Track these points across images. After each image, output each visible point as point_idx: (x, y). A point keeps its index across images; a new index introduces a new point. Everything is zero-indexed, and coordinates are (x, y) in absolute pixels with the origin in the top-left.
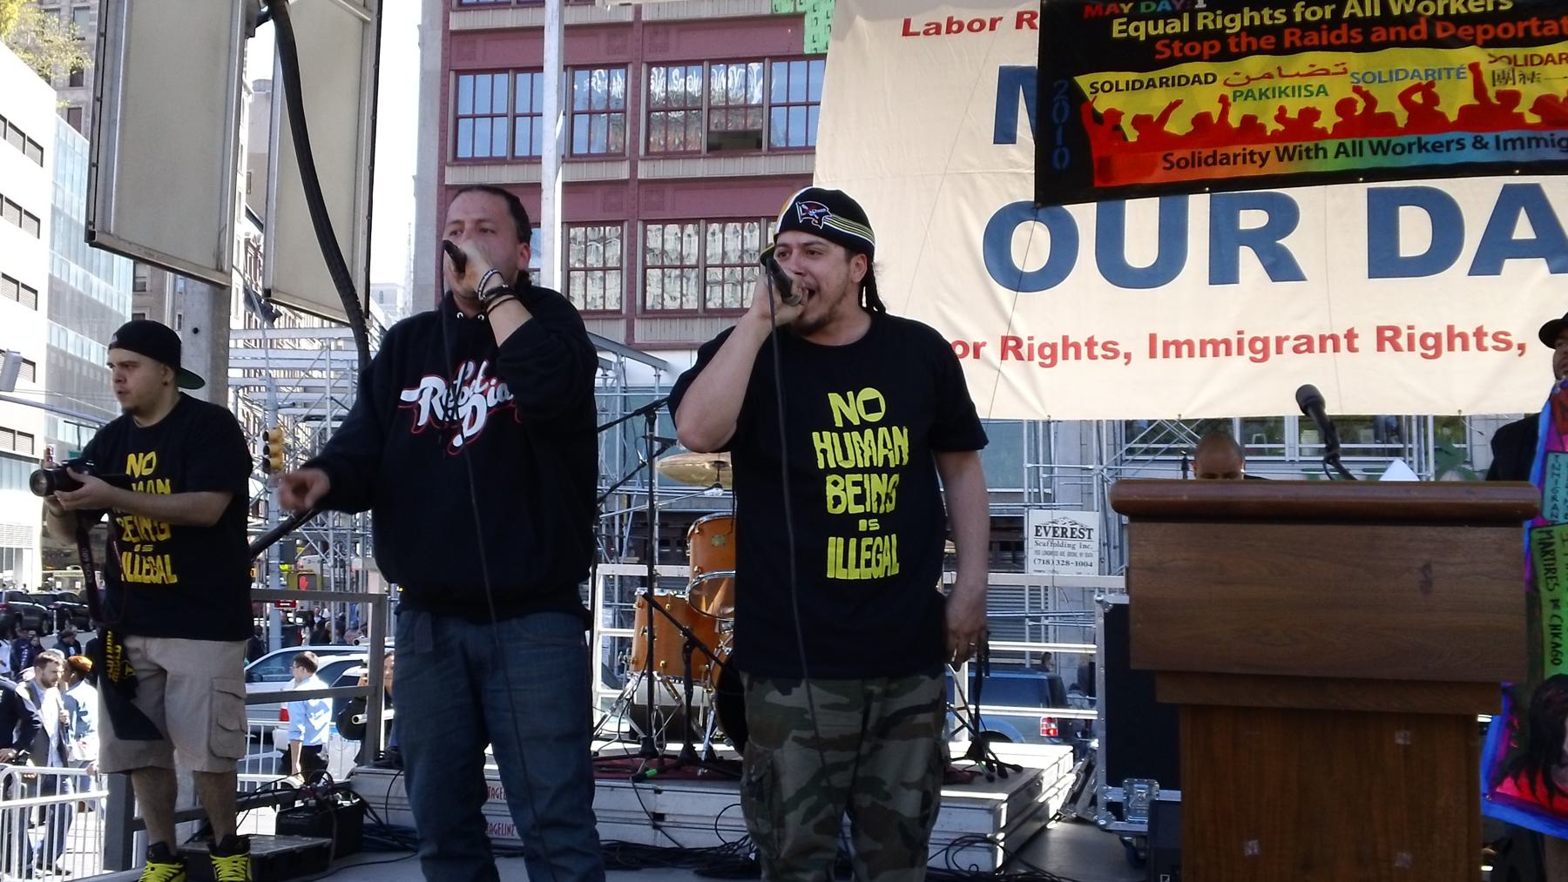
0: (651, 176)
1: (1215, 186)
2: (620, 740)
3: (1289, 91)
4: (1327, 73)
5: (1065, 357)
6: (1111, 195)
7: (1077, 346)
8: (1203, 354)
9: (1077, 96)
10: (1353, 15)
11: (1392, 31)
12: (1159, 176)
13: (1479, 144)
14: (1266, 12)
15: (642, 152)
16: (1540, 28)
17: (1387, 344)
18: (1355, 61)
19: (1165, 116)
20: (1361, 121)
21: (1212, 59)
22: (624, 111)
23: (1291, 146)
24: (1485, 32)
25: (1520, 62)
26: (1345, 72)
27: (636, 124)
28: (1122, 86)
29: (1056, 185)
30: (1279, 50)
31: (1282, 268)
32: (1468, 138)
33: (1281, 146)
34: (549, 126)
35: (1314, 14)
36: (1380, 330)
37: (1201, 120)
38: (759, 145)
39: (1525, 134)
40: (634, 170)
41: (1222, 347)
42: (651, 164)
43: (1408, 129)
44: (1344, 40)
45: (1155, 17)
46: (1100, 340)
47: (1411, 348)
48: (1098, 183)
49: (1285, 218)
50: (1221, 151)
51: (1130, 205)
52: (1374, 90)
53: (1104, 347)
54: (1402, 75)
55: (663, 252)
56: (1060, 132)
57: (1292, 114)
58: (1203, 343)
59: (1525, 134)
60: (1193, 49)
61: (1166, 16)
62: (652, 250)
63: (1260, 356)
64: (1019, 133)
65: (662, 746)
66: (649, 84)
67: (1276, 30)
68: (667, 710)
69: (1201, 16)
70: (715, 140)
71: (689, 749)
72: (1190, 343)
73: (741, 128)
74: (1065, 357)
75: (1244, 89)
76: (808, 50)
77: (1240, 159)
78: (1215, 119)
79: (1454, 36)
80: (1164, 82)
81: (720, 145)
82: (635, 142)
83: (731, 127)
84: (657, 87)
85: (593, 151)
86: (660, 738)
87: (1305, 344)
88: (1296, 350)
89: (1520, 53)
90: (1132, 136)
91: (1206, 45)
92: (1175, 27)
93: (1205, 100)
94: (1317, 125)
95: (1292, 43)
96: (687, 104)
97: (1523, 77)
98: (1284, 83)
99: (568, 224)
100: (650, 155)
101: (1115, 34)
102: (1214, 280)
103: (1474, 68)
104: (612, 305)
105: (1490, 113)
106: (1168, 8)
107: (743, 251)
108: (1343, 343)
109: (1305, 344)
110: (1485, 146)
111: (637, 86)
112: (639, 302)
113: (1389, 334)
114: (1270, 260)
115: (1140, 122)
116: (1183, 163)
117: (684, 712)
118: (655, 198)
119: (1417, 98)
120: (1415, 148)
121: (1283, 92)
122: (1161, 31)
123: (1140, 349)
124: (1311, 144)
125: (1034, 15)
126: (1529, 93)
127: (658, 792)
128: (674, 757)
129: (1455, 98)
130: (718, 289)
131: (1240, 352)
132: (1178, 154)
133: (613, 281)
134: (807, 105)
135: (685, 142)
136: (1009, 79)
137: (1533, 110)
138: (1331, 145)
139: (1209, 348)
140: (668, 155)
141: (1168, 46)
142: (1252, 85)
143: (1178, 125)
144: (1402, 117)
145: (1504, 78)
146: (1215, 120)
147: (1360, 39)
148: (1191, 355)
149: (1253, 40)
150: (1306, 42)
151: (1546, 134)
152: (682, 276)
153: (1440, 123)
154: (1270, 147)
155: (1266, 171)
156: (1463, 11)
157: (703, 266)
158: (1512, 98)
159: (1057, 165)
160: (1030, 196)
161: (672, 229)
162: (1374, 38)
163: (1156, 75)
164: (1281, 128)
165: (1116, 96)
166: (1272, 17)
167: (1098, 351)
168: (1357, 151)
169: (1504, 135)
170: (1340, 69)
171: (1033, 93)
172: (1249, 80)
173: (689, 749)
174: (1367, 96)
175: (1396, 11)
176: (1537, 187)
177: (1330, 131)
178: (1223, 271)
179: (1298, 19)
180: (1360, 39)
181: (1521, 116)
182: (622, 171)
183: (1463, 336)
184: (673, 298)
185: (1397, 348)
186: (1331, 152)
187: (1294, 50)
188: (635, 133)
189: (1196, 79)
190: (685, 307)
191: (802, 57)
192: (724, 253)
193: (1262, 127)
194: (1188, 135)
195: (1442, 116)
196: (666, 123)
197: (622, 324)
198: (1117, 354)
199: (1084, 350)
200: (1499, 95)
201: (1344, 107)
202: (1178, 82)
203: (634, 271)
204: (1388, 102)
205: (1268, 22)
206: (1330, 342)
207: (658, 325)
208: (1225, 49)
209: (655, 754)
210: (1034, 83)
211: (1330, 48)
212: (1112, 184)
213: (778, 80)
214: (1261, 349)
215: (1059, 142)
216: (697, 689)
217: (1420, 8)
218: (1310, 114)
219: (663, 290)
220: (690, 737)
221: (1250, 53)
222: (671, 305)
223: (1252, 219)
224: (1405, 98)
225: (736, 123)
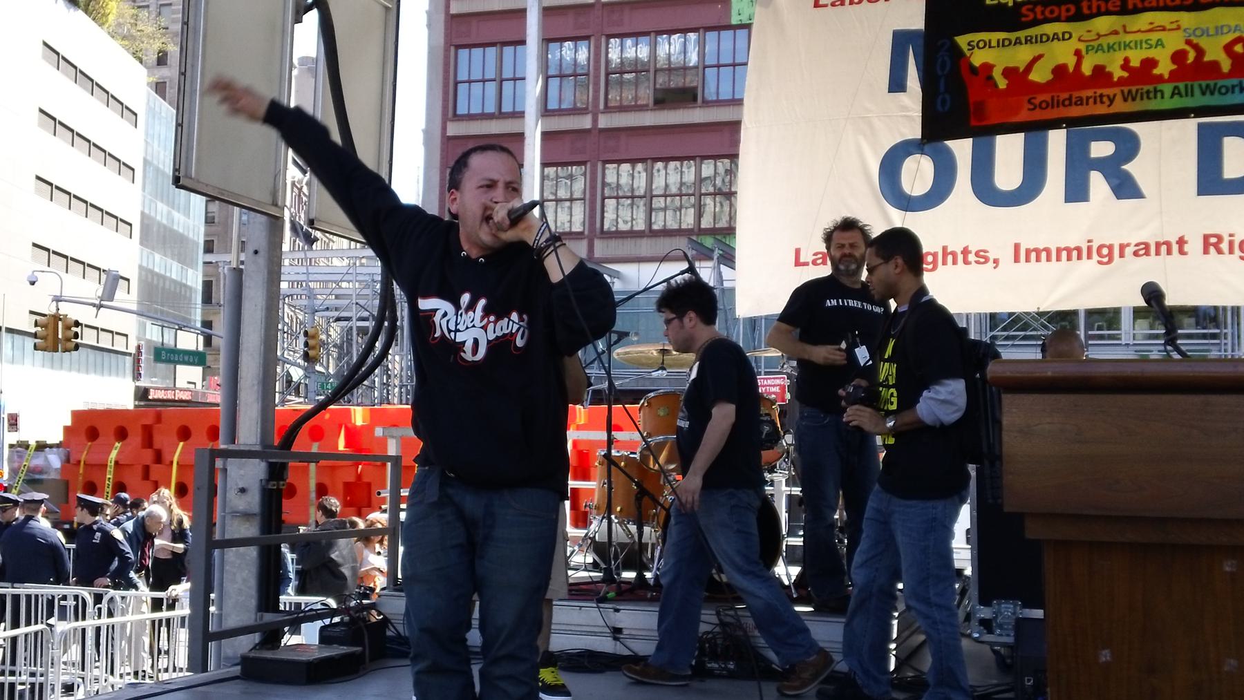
0: (609, 125)
1: (1070, 123)
2: (586, 570)
3: (1132, 45)
4: (1164, 29)
5: (944, 263)
7: (954, 254)
8: (1059, 259)
9: (957, 53)
12: (1024, 116)
15: (602, 106)
17: (1212, 249)
18: (1187, 19)
19: (1029, 67)
20: (1192, 68)
21: (1069, 19)
23: (1134, 89)
26: (1178, 28)
27: (597, 84)
28: (994, 43)
29: (941, 123)
31: (1125, 188)
33: (1126, 90)
34: (530, 85)
36: (1206, 238)
37: (1060, 70)
38: (695, 99)
40: (595, 121)
41: (1075, 253)
43: (1230, 75)
46: (973, 249)
47: (1231, 251)
48: (973, 123)
49: (1129, 147)
50: (1076, 94)
52: (1203, 42)
53: (977, 254)
54: (1225, 30)
55: (618, 186)
57: (1135, 63)
58: (1059, 251)
60: (1052, 12)
62: (609, 185)
63: (1106, 260)
65: (619, 575)
66: (607, 53)
68: (623, 546)
70: (660, 96)
71: (641, 577)
72: (1048, 251)
73: (680, 85)
74: (944, 263)
75: (1095, 44)
76: (734, 21)
77: (1091, 101)
78: (1071, 69)
80: (1028, 40)
81: (665, 99)
82: (596, 98)
83: (672, 85)
84: (614, 55)
85: (563, 107)
86: (617, 568)
87: (1143, 249)
88: (1136, 254)
90: (1002, 84)
91: (1063, 8)
93: (1063, 54)
94: (1156, 71)
95: (1135, 5)
96: (637, 67)
98: (1129, 38)
99: (544, 165)
100: (608, 109)
102: (1068, 199)
104: (577, 228)
107: (682, 184)
108: (1175, 248)
109: (1143, 249)
111: (598, 55)
112: (598, 225)
113: (1213, 240)
114: (1116, 182)
115: (1009, 72)
116: (1044, 105)
117: (637, 547)
120: (1237, 90)
121: (1127, 46)
123: (1007, 255)
124: (1151, 88)
127: (617, 610)
128: (629, 583)
130: (661, 214)
131: (1089, 257)
132: (1040, 98)
133: (578, 209)
134: (734, 65)
135: (636, 98)
136: (901, 40)
138: (1167, 88)
139: (1064, 254)
140: (622, 109)
141: (1032, 10)
142: (1101, 41)
143: (1040, 75)
144: (1226, 65)
146: (1071, 69)
148: (1049, 259)
152: (632, 205)
154: (1116, 90)
155: (1112, 110)
157: (649, 196)
159: (939, 108)
160: (918, 134)
161: (626, 167)
163: (1022, 34)
164: (1125, 74)
165: (988, 51)
167: (971, 257)
168: (1189, 92)
170: (1174, 26)
171: (921, 50)
172: (1099, 36)
173: (641, 577)
174: (1196, 47)
177: (1166, 76)
178: (1076, 191)
182: (585, 122)
184: (625, 222)
185: (1220, 252)
186: (1168, 93)
187: (1136, 11)
188: (596, 91)
189: (1056, 37)
190: (635, 228)
191: (729, 27)
192: (667, 186)
193: (1110, 75)
194: (1049, 83)
196: (621, 83)
197: (584, 243)
198: (987, 260)
199: (960, 257)
201: (1178, 57)
202: (1040, 39)
203: (594, 201)
204: (1215, 52)
206: (1163, 247)
207: (613, 243)
209: (614, 581)
210: (921, 42)
212: (984, 123)
213: (710, 47)
214: (1106, 254)
215: (942, 89)
216: (647, 529)
218: (1150, 63)
219: (617, 216)
220: (641, 567)
221: (1099, 14)
222: (623, 227)
223: (1101, 149)
224: (1228, 48)
225: (676, 82)
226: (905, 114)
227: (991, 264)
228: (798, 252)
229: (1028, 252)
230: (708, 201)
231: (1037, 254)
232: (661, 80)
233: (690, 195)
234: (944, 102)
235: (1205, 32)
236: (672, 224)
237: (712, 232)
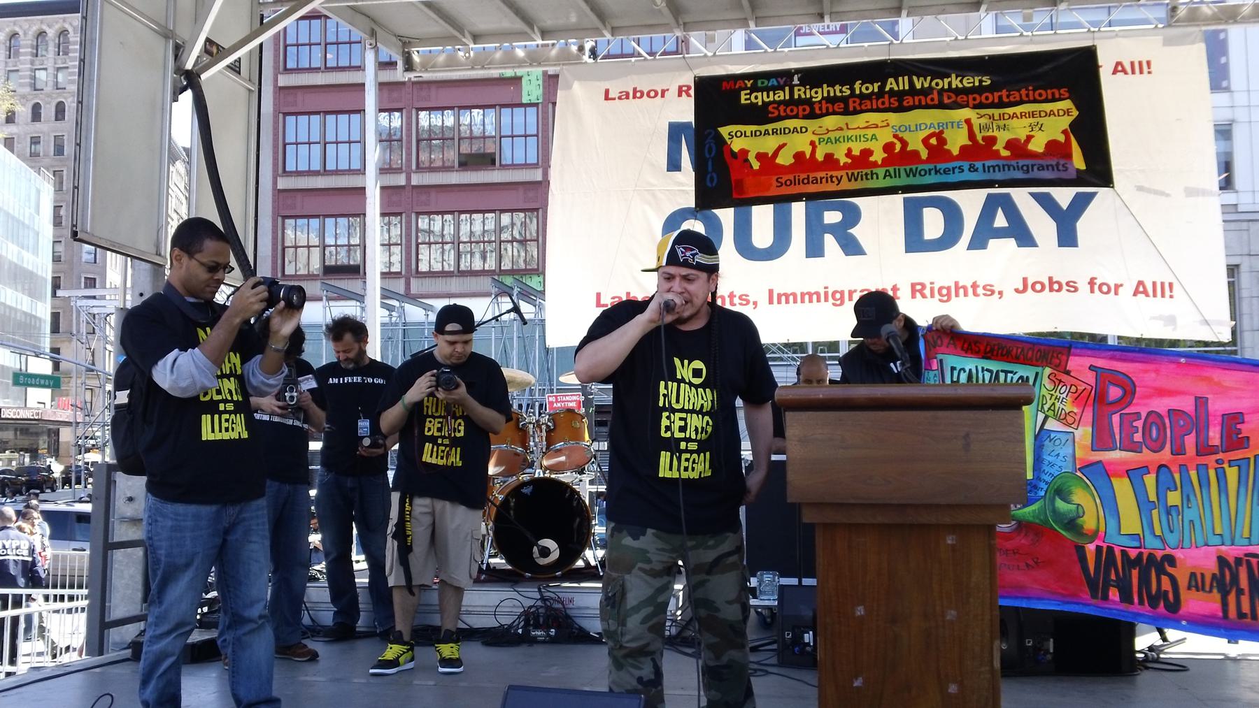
1: (809, 197)
4: (877, 127)
6: (742, 202)
8: (803, 301)
9: (720, 141)
10: (891, 89)
11: (916, 98)
13: (973, 169)
14: (838, 87)
15: (414, 167)
16: (1008, 97)
17: (918, 294)
18: (893, 118)
20: (899, 156)
21: (805, 117)
22: (400, 140)
24: (974, 99)
25: (997, 117)
28: (748, 134)
30: (846, 112)
31: (851, 247)
32: (966, 165)
35: (867, 89)
36: (913, 285)
37: (799, 156)
38: (493, 163)
39: (1000, 163)
42: (420, 175)
43: (928, 161)
44: (887, 105)
45: (767, 89)
46: (737, 294)
47: (932, 296)
48: (735, 196)
49: (853, 216)
50: (812, 175)
51: (755, 208)
52: (906, 136)
53: (740, 298)
55: (430, 232)
56: (710, 163)
57: (856, 152)
58: (803, 295)
59: (1000, 163)
61: (774, 89)
64: (683, 165)
67: (844, 100)
69: (796, 89)
70: (463, 159)
72: (794, 295)
75: (826, 137)
78: (808, 156)
79: (955, 102)
80: (775, 132)
81: (468, 162)
82: (409, 160)
89: (996, 112)
90: (756, 165)
91: (801, 108)
92: (781, 96)
93: (800, 143)
94: (872, 159)
96: (445, 137)
97: (999, 127)
98: (850, 133)
101: (743, 101)
103: (968, 122)
105: (978, 150)
106: (775, 83)
107: (484, 231)
110: (976, 170)
113: (919, 287)
115: (760, 157)
118: (423, 198)
119: (933, 141)
122: (771, 99)
125: (689, 88)
126: (1003, 137)
129: (957, 140)
131: (826, 300)
132: (785, 178)
136: (675, 131)
137: (1006, 148)
139: (807, 297)
141: (777, 108)
142: (830, 135)
143: (785, 159)
144: (924, 154)
145: (987, 128)
146: (808, 156)
147: (896, 104)
148: (795, 301)
149: (830, 106)
150: (863, 107)
151: (1013, 163)
153: (946, 156)
154: (843, 173)
155: (840, 188)
156: (960, 86)
157: (457, 242)
158: (992, 140)
159: (709, 184)
160: (693, 205)
162: (905, 103)
163: (770, 127)
165: (743, 140)
166: (841, 91)
169: (988, 163)
175: (918, 86)
176: (1008, 196)
178: (814, 249)
179: (858, 92)
180: (896, 104)
181: (998, 151)
183: (965, 288)
185: (924, 296)
186: (881, 176)
187: (855, 112)
188: (409, 154)
193: (837, 161)
195: (949, 152)
198: (748, 302)
200: (983, 138)
201: (888, 148)
202: (784, 131)
204: (915, 143)
205: (838, 94)
208: (812, 112)
210: (692, 133)
211: (878, 110)
215: (710, 169)
217: (933, 84)
218: (867, 153)
223: (832, 217)
224: (925, 141)
225: (476, 148)
226: (682, 187)
227: (751, 305)
228: (598, 295)
229: (779, 296)
230: (509, 246)
231: (786, 297)
232: (465, 148)
233: (490, 242)
234: (712, 180)
235: (908, 129)
236: (478, 265)
237: (512, 272)
